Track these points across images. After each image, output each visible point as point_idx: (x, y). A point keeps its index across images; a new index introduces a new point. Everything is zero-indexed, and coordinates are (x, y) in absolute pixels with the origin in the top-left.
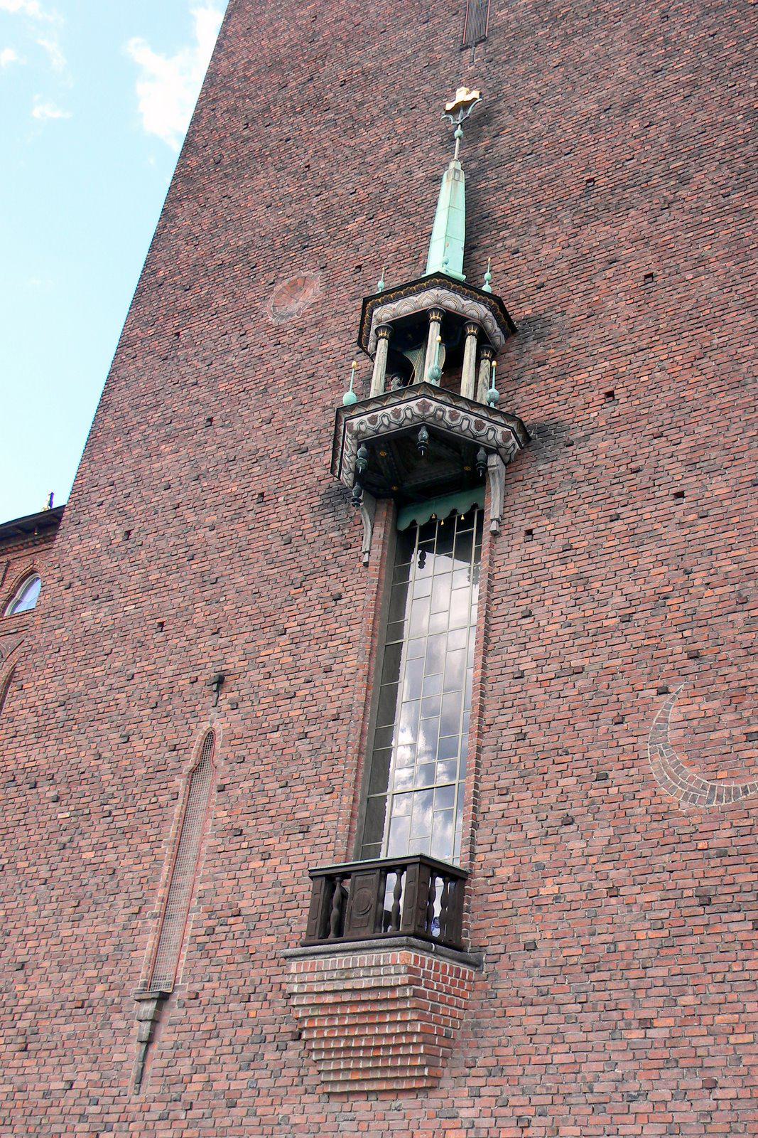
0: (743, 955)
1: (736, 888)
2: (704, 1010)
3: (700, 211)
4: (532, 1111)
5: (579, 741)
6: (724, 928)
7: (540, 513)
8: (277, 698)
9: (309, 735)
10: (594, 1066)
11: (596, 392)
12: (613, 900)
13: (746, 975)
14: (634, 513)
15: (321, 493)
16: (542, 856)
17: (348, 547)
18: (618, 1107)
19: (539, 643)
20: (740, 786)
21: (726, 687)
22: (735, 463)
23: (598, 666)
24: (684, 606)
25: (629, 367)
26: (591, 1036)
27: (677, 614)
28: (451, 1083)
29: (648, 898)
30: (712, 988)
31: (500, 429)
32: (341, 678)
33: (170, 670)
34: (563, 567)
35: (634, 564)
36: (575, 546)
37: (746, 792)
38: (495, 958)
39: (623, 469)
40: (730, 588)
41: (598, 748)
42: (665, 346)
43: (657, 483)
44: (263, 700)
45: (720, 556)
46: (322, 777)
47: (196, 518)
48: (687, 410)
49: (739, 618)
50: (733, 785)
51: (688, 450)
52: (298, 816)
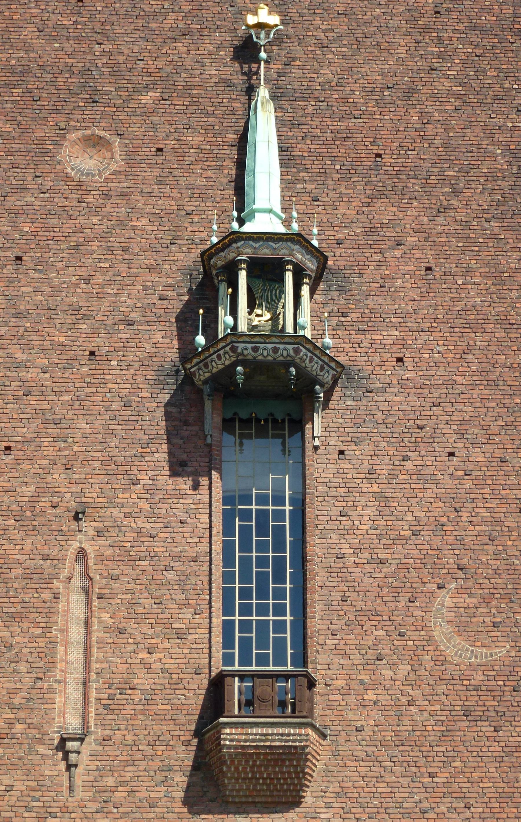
0: (488, 744)
1: (485, 708)
2: (466, 770)
3: (467, 225)
4: (366, 816)
5: (386, 609)
6: (478, 729)
7: (350, 439)
8: (140, 535)
9: (174, 568)
10: (403, 795)
11: (390, 355)
12: (412, 708)
13: (490, 754)
14: (420, 458)
15: (156, 368)
16: (364, 677)
17: (186, 423)
18: (417, 816)
19: (353, 536)
20: (488, 652)
21: (481, 591)
22: (490, 442)
23: (397, 561)
24: (455, 533)
25: (415, 342)
26: (400, 779)
27: (450, 538)
28: (313, 800)
29: (433, 708)
30: (471, 759)
31: (332, 372)
32: (196, 530)
33: (28, 491)
34: (369, 485)
35: (421, 495)
36: (378, 472)
37: (492, 656)
38: (336, 733)
39: (411, 422)
40: (486, 528)
41: (400, 615)
42: (442, 334)
43: (436, 440)
44: (127, 534)
45: (479, 505)
46: (191, 601)
47: (25, 356)
48: (457, 392)
49: (490, 549)
50: (484, 651)
51: (458, 423)
52: (174, 626)
